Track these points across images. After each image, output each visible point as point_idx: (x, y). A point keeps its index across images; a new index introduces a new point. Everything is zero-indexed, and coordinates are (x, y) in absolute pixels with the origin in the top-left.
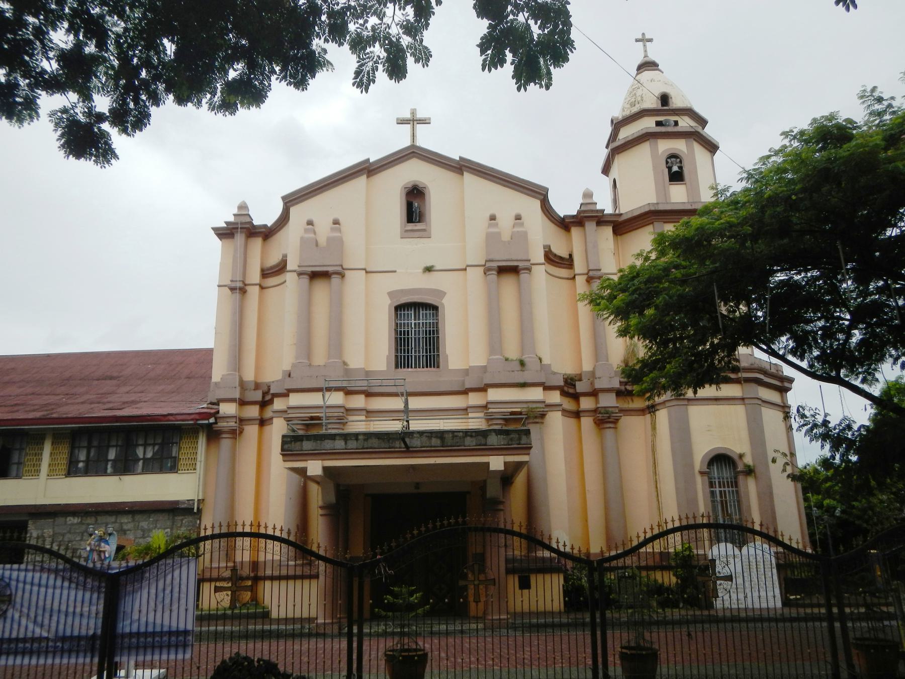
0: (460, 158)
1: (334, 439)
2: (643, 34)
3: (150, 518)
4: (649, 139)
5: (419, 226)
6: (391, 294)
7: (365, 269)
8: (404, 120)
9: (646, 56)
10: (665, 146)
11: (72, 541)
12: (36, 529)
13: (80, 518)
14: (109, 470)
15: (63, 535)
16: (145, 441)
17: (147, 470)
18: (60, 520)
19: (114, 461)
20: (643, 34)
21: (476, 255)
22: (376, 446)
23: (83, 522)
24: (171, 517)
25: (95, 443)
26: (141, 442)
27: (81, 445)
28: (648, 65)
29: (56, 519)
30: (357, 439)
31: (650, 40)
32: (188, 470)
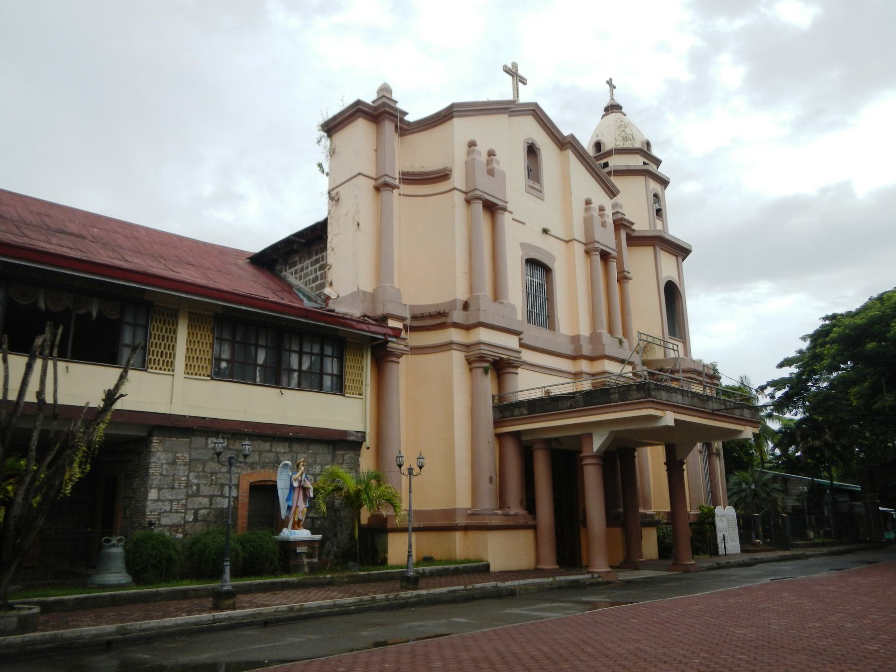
0: (572, 136)
1: (677, 393)
2: (611, 79)
3: (308, 450)
4: (645, 175)
5: (537, 186)
6: (523, 246)
7: (512, 213)
8: (511, 71)
9: (612, 99)
10: (654, 186)
11: (216, 474)
12: (165, 451)
13: (226, 440)
14: (258, 380)
15: (204, 463)
16: (301, 347)
17: (299, 388)
18: (198, 441)
19: (264, 366)
20: (611, 79)
21: (579, 234)
22: (698, 405)
23: (231, 447)
24: (331, 451)
25: (238, 339)
26: (295, 347)
27: (223, 337)
28: (613, 108)
29: (193, 438)
30: (688, 396)
31: (614, 87)
32: (353, 394)
